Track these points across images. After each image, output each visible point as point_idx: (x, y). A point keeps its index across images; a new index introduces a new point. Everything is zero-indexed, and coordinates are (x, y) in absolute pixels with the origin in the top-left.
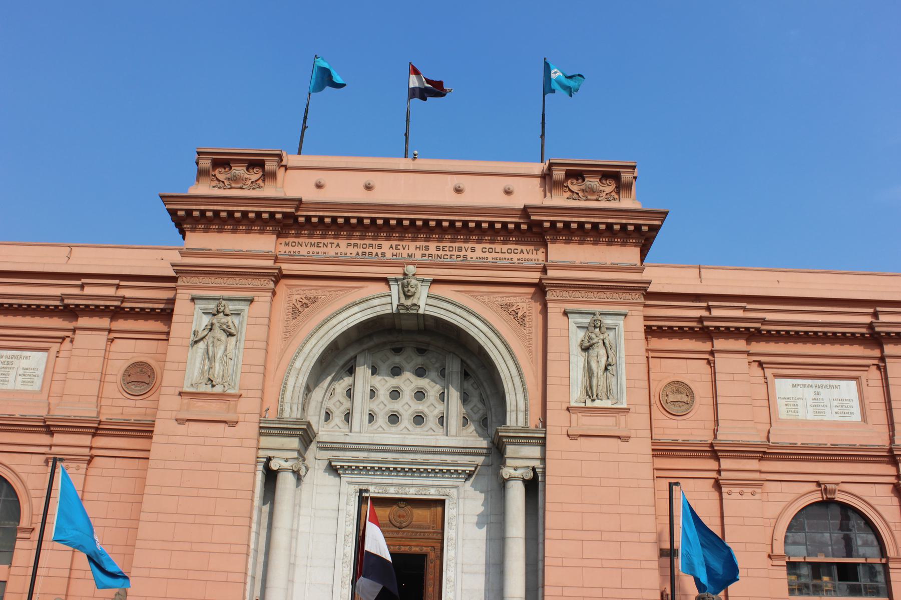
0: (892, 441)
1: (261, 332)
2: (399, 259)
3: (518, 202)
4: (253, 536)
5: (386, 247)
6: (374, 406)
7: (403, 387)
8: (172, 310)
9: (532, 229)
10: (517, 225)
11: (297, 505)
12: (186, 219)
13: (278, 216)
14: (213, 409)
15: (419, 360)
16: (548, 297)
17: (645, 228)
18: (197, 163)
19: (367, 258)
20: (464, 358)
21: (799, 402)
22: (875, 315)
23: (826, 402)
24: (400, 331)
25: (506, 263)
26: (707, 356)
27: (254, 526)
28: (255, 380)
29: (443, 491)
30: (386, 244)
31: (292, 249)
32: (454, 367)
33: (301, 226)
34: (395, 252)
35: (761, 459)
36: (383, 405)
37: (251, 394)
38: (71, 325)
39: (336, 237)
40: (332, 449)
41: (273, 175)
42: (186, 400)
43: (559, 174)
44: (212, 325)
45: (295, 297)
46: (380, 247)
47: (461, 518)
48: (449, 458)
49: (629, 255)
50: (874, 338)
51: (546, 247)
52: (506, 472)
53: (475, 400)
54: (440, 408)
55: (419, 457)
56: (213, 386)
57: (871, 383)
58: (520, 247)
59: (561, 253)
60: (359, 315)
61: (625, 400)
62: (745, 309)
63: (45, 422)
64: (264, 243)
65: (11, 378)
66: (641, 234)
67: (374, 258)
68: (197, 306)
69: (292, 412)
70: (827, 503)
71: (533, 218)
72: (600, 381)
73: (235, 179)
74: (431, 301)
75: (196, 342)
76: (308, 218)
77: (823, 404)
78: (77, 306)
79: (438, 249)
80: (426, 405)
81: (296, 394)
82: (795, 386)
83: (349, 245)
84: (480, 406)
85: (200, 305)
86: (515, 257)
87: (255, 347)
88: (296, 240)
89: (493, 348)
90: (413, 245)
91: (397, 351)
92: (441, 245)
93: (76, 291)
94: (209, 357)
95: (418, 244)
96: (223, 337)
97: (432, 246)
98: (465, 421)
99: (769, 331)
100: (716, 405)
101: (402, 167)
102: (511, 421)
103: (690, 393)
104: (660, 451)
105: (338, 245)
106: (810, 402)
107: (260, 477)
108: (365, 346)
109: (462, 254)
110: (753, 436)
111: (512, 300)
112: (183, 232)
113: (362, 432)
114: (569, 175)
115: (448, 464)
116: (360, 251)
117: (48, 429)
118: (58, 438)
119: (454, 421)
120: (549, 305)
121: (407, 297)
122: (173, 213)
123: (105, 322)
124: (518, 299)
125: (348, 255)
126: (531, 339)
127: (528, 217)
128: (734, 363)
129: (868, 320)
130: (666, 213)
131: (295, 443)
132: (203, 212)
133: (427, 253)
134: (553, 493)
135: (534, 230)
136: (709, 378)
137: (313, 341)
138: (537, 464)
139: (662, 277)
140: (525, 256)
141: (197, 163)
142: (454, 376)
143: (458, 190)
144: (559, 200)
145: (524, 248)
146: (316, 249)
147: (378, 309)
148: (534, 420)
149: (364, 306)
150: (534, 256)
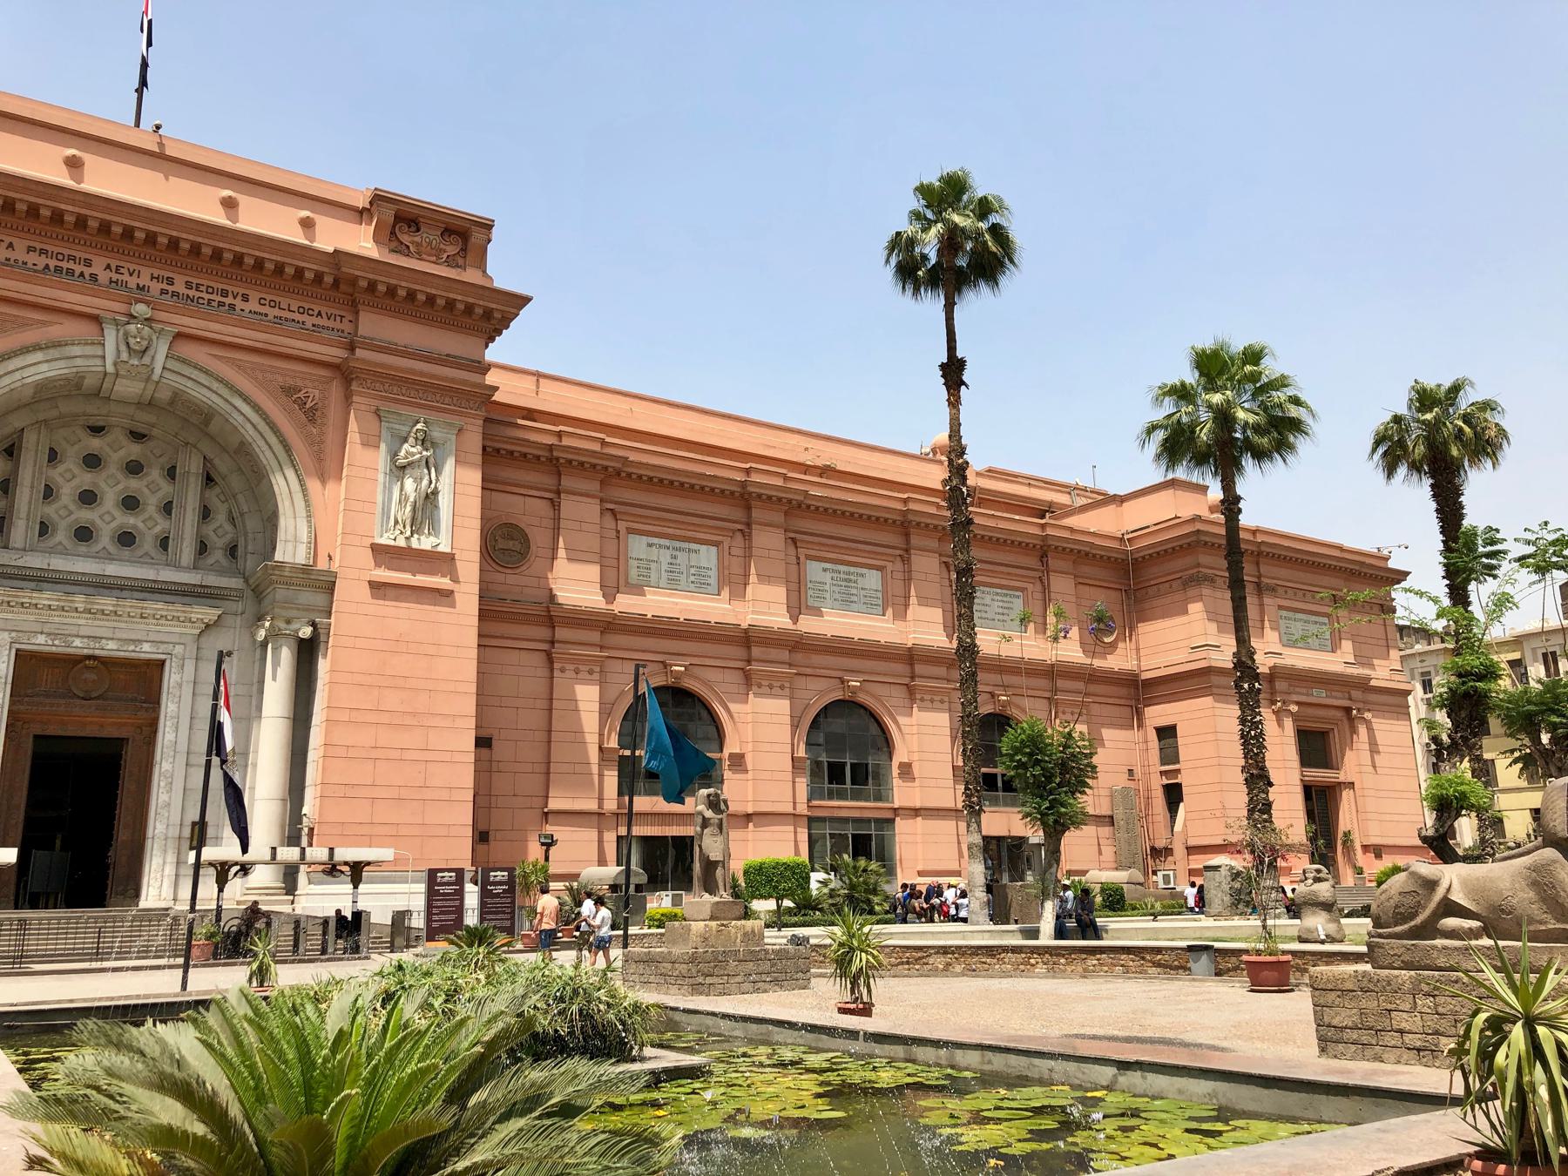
6: (50, 510)
7: (103, 485)
9: (338, 283)
10: (319, 278)
15: (134, 450)
16: (354, 387)
20: (210, 455)
21: (653, 566)
23: (683, 568)
29: (163, 648)
32: (192, 466)
34: (115, 277)
36: (65, 511)
46: (88, 263)
51: (357, 313)
54: (161, 525)
57: (735, 551)
60: (44, 367)
62: (603, 443)
74: (171, 364)
79: (188, 285)
80: (142, 518)
82: (650, 545)
83: (30, 249)
84: (228, 527)
86: (310, 321)
89: (265, 448)
90: (146, 273)
91: (97, 430)
92: (195, 281)
98: (203, 548)
99: (629, 475)
103: (525, 540)
105: (11, 245)
106: (665, 567)
109: (228, 301)
111: (300, 383)
116: (52, 263)
120: (355, 398)
125: (30, 265)
126: (322, 442)
127: (338, 267)
128: (581, 510)
130: (526, 300)
133: (170, 288)
135: (343, 287)
136: (548, 523)
142: (192, 479)
145: (324, 310)
147: (79, 362)
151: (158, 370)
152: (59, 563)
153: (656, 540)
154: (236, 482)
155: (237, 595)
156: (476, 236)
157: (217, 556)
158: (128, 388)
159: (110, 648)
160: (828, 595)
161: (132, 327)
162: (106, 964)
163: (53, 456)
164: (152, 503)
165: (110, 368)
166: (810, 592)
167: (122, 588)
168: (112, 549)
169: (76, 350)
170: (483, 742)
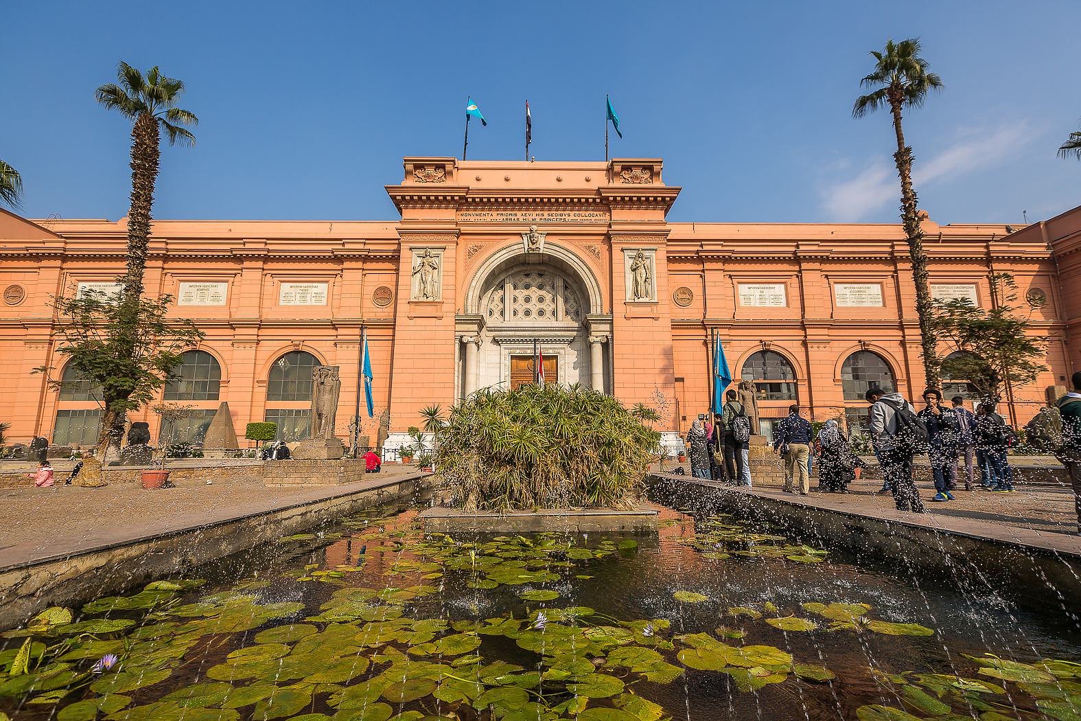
0: (803, 316)
1: (451, 266)
2: (527, 222)
3: (594, 185)
4: (456, 378)
5: (520, 215)
6: (516, 306)
7: (531, 295)
8: (399, 256)
9: (603, 202)
10: (594, 200)
11: (478, 361)
12: (401, 202)
13: (456, 198)
14: (429, 310)
15: (540, 280)
17: (668, 199)
18: (405, 167)
19: (509, 222)
21: (752, 297)
22: (797, 246)
24: (529, 264)
25: (588, 222)
26: (700, 273)
27: (456, 373)
28: (451, 294)
30: (519, 214)
31: (466, 218)
32: (559, 283)
33: (470, 204)
35: (730, 329)
36: (521, 306)
37: (449, 301)
38: (340, 267)
39: (490, 210)
40: (495, 331)
41: (451, 173)
42: (413, 306)
43: (617, 168)
44: (423, 263)
45: (469, 246)
46: (516, 215)
47: (567, 365)
48: (559, 333)
49: (657, 215)
50: (797, 260)
52: (592, 339)
53: (572, 301)
54: (553, 306)
55: (542, 333)
56: (427, 298)
58: (595, 213)
59: (619, 215)
61: (656, 297)
62: (722, 245)
63: (332, 322)
64: (449, 214)
65: (308, 299)
66: (664, 203)
67: (513, 222)
69: (472, 310)
70: (764, 353)
71: (603, 195)
72: (641, 288)
73: (428, 176)
75: (415, 273)
76: (474, 199)
77: (764, 298)
78: (342, 255)
81: (474, 301)
82: (749, 288)
85: (415, 252)
86: (593, 219)
87: (448, 275)
88: (467, 212)
91: (527, 275)
92: (550, 212)
93: (341, 247)
94: (423, 281)
95: (538, 212)
96: (431, 270)
97: (546, 213)
98: (567, 313)
99: (736, 258)
101: (526, 167)
102: (593, 311)
103: (691, 294)
104: (676, 325)
106: (758, 297)
107: (457, 346)
108: (509, 273)
110: (726, 316)
111: (592, 243)
112: (400, 210)
113: (511, 321)
114: (624, 168)
115: (559, 336)
117: (334, 326)
118: (340, 331)
119: (561, 313)
121: (533, 244)
122: (393, 198)
123: (359, 265)
124: (595, 243)
128: (716, 276)
129: (793, 249)
131: (475, 327)
132: (412, 197)
134: (618, 349)
137: (481, 270)
138: (608, 334)
139: (679, 230)
140: (599, 218)
141: (405, 167)
143: (559, 180)
144: (617, 183)
145: (598, 213)
146: (479, 218)
148: (606, 309)
150: (604, 218)
154: (574, 286)
160: (848, 300)
163: (515, 288)
166: (837, 300)
169: (516, 247)
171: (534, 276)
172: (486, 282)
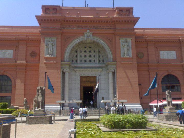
6: (81, 59)
9: (113, 22)
10: (110, 22)
15: (90, 49)
20: (99, 48)
21: (164, 55)
24: (86, 43)
32: (97, 50)
54: (94, 59)
60: (78, 41)
62: (154, 37)
68: (46, 40)
78: (19, 40)
79: (94, 26)
82: (164, 52)
84: (102, 58)
91: (85, 47)
96: (52, 46)
98: (99, 61)
100: (148, 56)
131: (68, 66)
149: (79, 39)
151: (91, 37)
152: (83, 65)
153: (164, 51)
155: (105, 67)
156: (131, 10)
157: (101, 62)
158: (88, 41)
159: (90, 75)
161: (88, 34)
162: (93, 115)
163: (81, 52)
164: (93, 56)
165: (86, 39)
167: (90, 67)
168: (89, 62)
170: (140, 85)
171: (88, 48)
172: (71, 50)
